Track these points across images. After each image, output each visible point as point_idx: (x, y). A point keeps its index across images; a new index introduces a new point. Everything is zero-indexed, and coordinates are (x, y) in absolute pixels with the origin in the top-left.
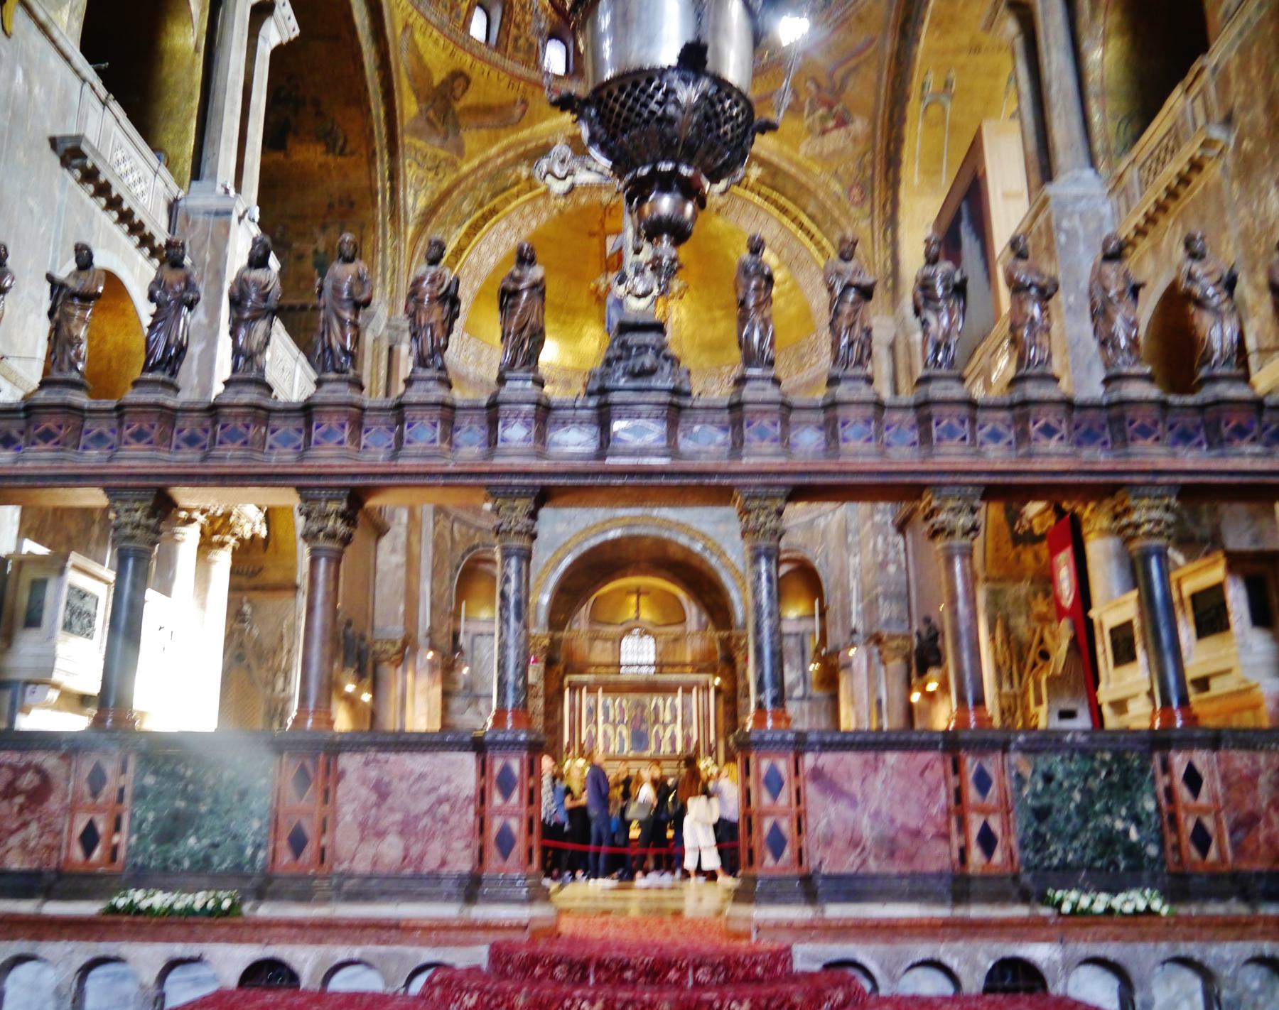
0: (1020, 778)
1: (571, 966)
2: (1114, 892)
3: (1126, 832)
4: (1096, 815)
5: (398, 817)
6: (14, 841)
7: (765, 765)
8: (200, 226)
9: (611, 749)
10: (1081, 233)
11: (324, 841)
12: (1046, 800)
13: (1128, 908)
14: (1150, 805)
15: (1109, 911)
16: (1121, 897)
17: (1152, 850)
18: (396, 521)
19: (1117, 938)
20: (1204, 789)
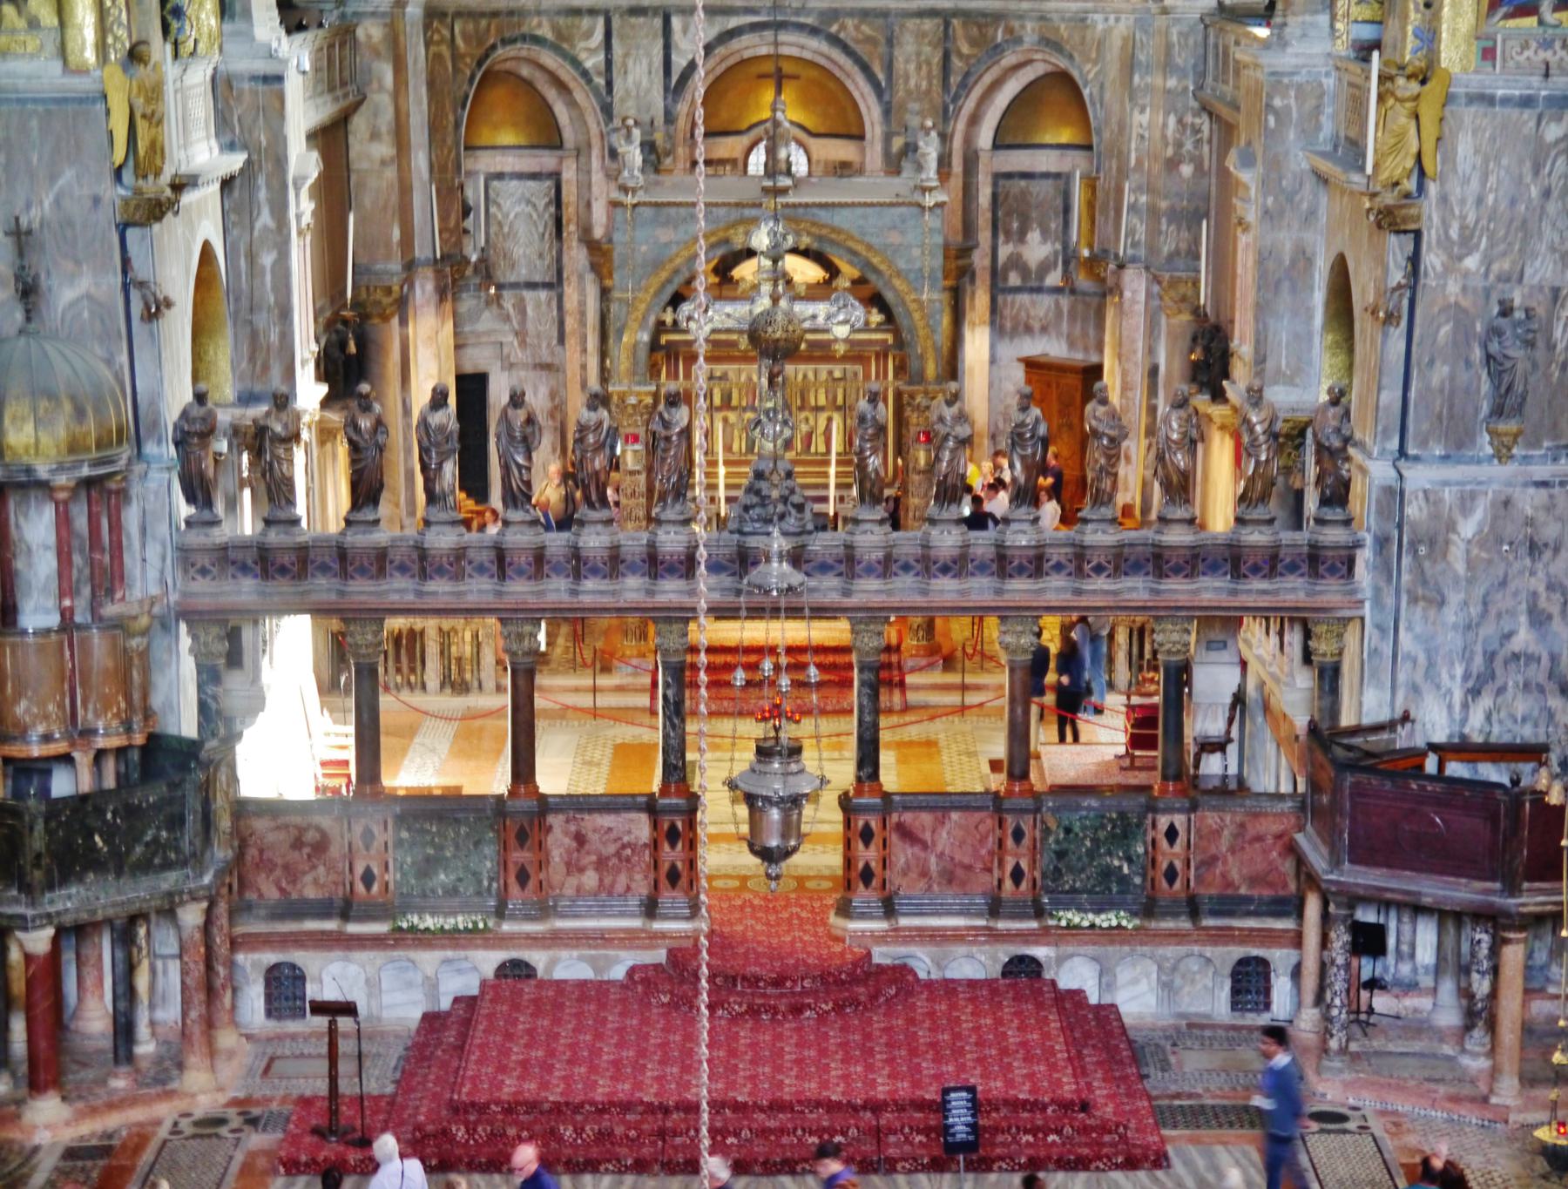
0: (1047, 831)
1: (726, 977)
2: (1098, 912)
3: (1120, 868)
4: (1100, 856)
5: (594, 858)
6: (308, 878)
7: (861, 823)
8: (247, 98)
9: (735, 447)
10: (1295, 115)
11: (542, 876)
12: (1065, 845)
13: (1105, 925)
14: (1140, 850)
15: (1092, 926)
16: (1103, 916)
17: (1138, 880)
18: (375, 85)
19: (1094, 944)
20: (1178, 841)
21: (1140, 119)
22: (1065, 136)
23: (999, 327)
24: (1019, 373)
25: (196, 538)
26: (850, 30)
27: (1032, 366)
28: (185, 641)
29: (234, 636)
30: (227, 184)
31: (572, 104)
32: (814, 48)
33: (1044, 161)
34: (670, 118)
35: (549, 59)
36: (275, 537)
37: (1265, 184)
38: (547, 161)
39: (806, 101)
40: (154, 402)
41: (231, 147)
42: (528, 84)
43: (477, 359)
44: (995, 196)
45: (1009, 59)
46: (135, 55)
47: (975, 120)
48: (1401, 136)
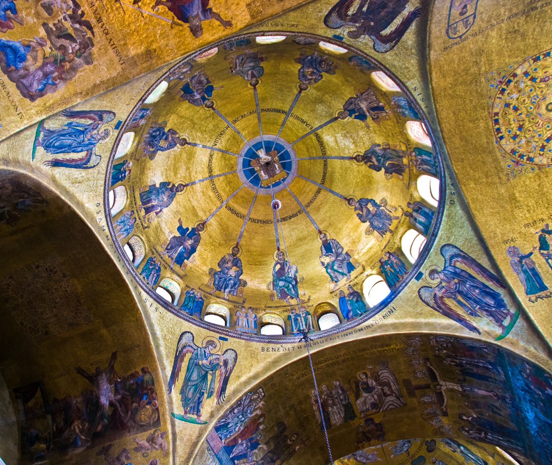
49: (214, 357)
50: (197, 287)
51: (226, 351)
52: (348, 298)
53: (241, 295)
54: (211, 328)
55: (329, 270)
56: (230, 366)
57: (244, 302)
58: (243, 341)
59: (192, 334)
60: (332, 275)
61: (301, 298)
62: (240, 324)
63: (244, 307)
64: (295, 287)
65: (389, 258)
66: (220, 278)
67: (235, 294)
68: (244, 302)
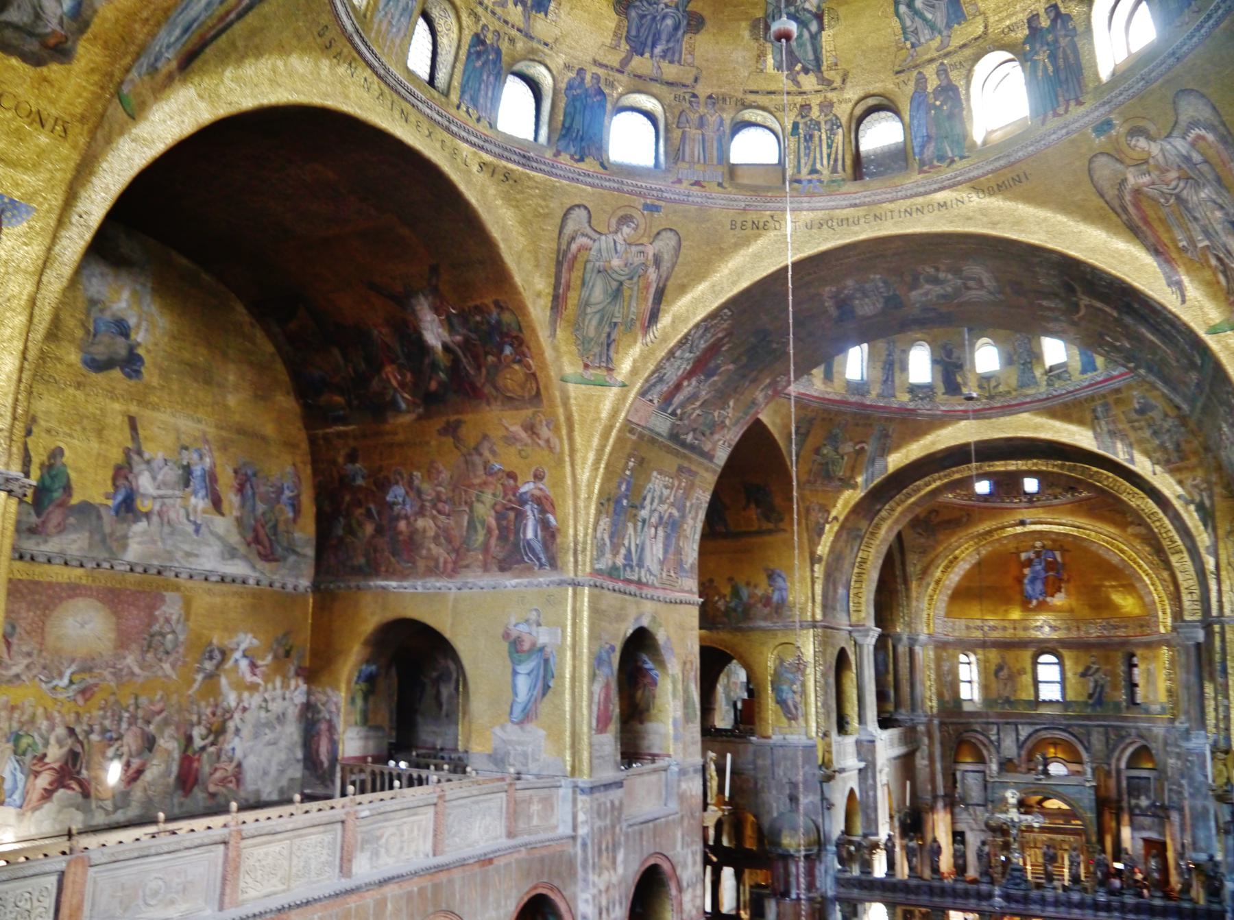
21: (1171, 761)
22: (1150, 765)
23: (1134, 827)
24: (1140, 844)
25: (841, 875)
26: (1076, 730)
27: (1146, 840)
28: (838, 907)
29: (855, 907)
30: (860, 770)
31: (988, 750)
32: (1064, 735)
33: (1144, 774)
34: (1019, 755)
35: (981, 737)
36: (864, 877)
37: (1190, 785)
38: (980, 767)
39: (1064, 752)
40: (830, 832)
41: (860, 760)
42: (974, 744)
43: (961, 827)
44: (1129, 785)
45: (1128, 741)
46: (826, 735)
47: (1119, 760)
48: (1221, 771)
49: (634, 249)
50: (589, 59)
51: (658, 234)
52: (931, 101)
53: (690, 61)
54: (626, 188)
55: (903, 9)
56: (665, 265)
57: (696, 80)
58: (693, 207)
59: (586, 208)
60: (908, 23)
61: (826, 75)
62: (687, 158)
63: (694, 96)
64: (815, 38)
65: (1054, 21)
66: (642, 17)
67: (676, 58)
68: (696, 80)
